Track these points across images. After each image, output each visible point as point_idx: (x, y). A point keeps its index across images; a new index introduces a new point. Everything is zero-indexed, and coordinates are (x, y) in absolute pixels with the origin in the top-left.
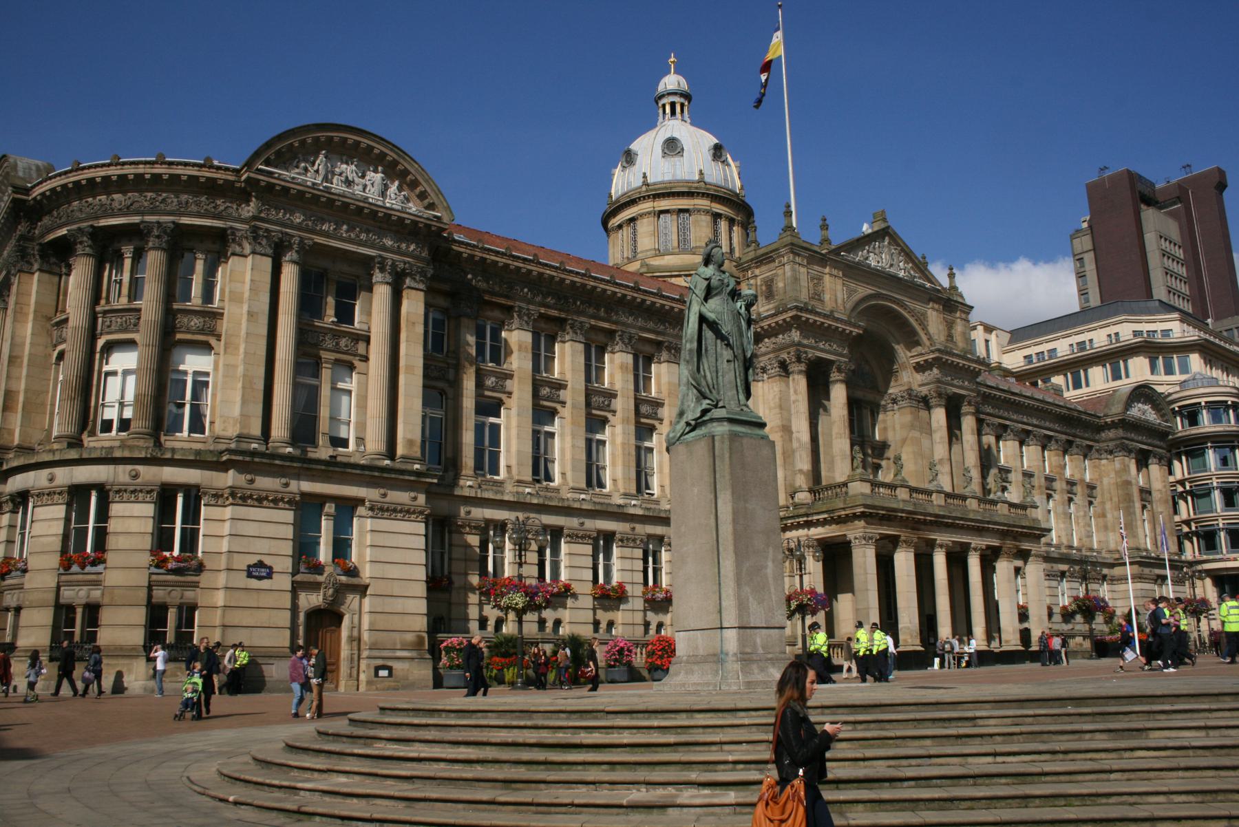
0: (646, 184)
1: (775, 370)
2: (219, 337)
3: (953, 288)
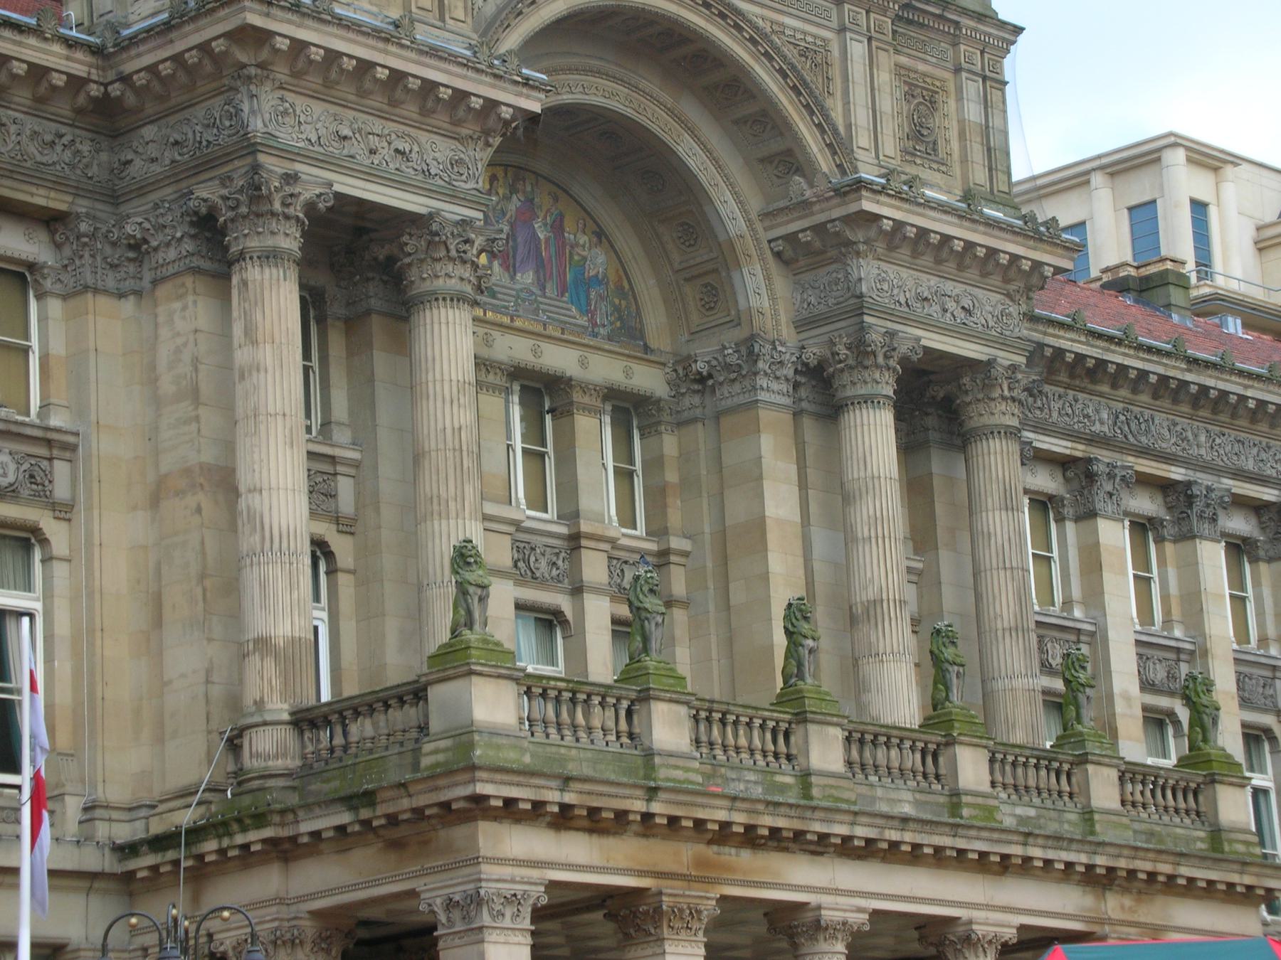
1: (177, 248)
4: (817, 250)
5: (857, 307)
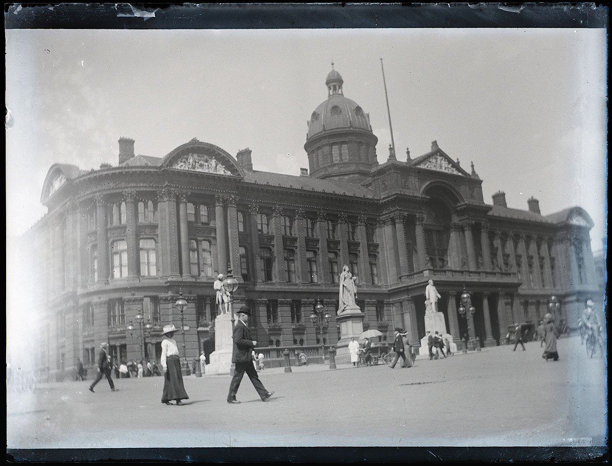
3: (474, 172)
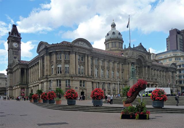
0: (110, 38)
2: (70, 63)
3: (149, 52)
4: (145, 62)
5: (146, 64)
